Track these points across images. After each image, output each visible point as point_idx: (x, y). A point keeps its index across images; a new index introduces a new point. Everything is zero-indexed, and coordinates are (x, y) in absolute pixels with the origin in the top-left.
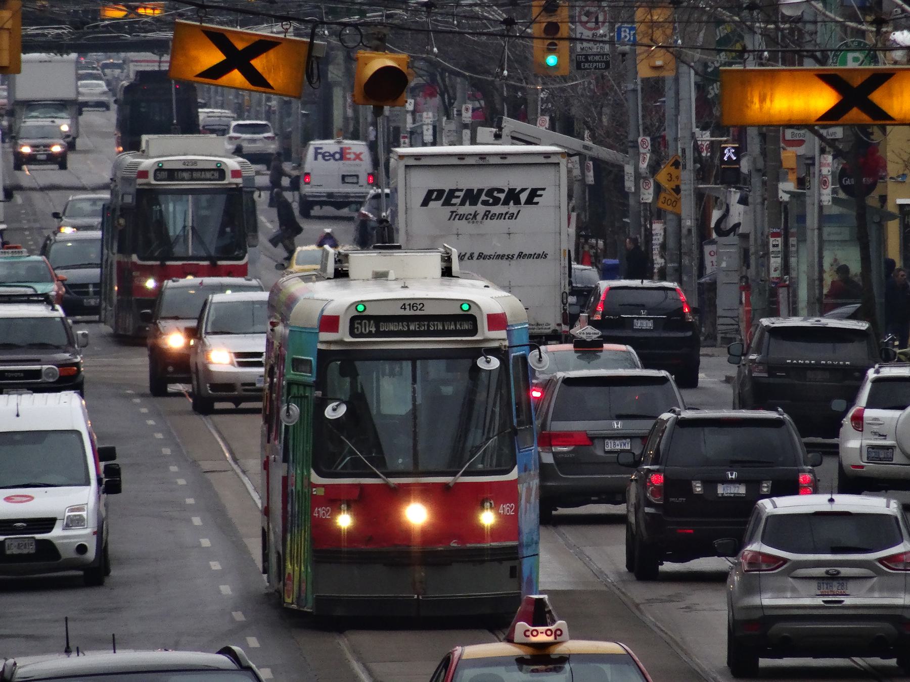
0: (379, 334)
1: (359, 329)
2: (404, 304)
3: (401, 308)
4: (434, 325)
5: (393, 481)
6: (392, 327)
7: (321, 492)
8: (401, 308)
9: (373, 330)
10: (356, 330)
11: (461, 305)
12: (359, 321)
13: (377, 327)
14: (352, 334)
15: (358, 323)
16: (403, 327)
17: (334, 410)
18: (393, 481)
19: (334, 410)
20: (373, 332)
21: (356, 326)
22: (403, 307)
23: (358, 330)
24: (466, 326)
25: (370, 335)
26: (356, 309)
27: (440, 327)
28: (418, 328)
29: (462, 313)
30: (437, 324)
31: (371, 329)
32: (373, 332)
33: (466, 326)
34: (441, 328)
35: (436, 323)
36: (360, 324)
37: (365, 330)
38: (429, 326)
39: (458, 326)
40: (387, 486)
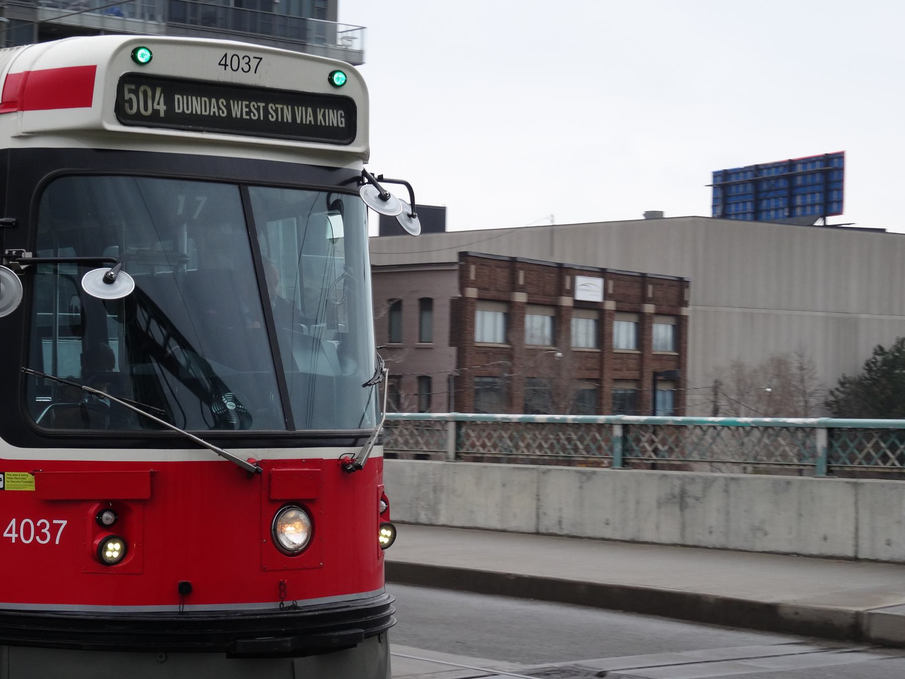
0: (174, 120)
1: (137, 105)
2: (226, 55)
3: (220, 64)
4: (276, 111)
5: (242, 454)
6: (196, 105)
7: (23, 482)
8: (220, 64)
9: (162, 108)
10: (127, 105)
11: (332, 74)
12: (133, 87)
13: (169, 102)
14: (121, 114)
15: (130, 91)
16: (219, 108)
17: (109, 280)
18: (242, 454)
19: (109, 280)
20: (162, 114)
21: (127, 96)
22: (223, 62)
23: (131, 108)
24: (335, 118)
25: (154, 120)
26: (134, 58)
27: (288, 117)
28: (248, 113)
29: (326, 89)
30: (282, 109)
31: (156, 107)
32: (162, 114)
33: (335, 118)
34: (290, 121)
35: (279, 106)
36: (136, 92)
37: (146, 109)
38: (266, 112)
39: (320, 117)
40: (232, 464)
